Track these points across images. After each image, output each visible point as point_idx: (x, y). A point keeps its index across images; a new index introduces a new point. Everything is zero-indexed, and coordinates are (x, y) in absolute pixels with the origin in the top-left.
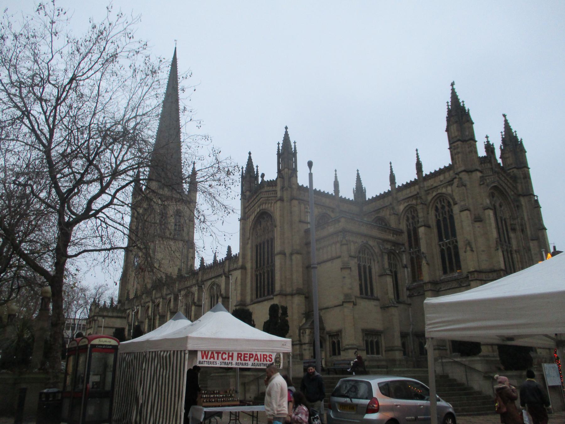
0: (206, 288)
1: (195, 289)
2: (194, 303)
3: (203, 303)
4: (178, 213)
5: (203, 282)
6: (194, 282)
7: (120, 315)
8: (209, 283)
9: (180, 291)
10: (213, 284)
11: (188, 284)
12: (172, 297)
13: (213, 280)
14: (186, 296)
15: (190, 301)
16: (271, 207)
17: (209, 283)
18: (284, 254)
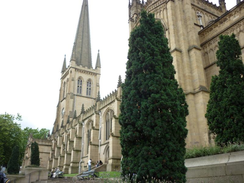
0: (102, 115)
1: (94, 118)
2: (93, 128)
3: (100, 127)
4: (89, 82)
5: (100, 110)
6: (94, 112)
7: (47, 144)
8: (105, 109)
9: (83, 121)
10: (108, 110)
11: (88, 115)
12: (78, 126)
13: (108, 107)
14: (88, 124)
15: (90, 127)
16: (160, 15)
17: (105, 109)
18: (180, 51)
